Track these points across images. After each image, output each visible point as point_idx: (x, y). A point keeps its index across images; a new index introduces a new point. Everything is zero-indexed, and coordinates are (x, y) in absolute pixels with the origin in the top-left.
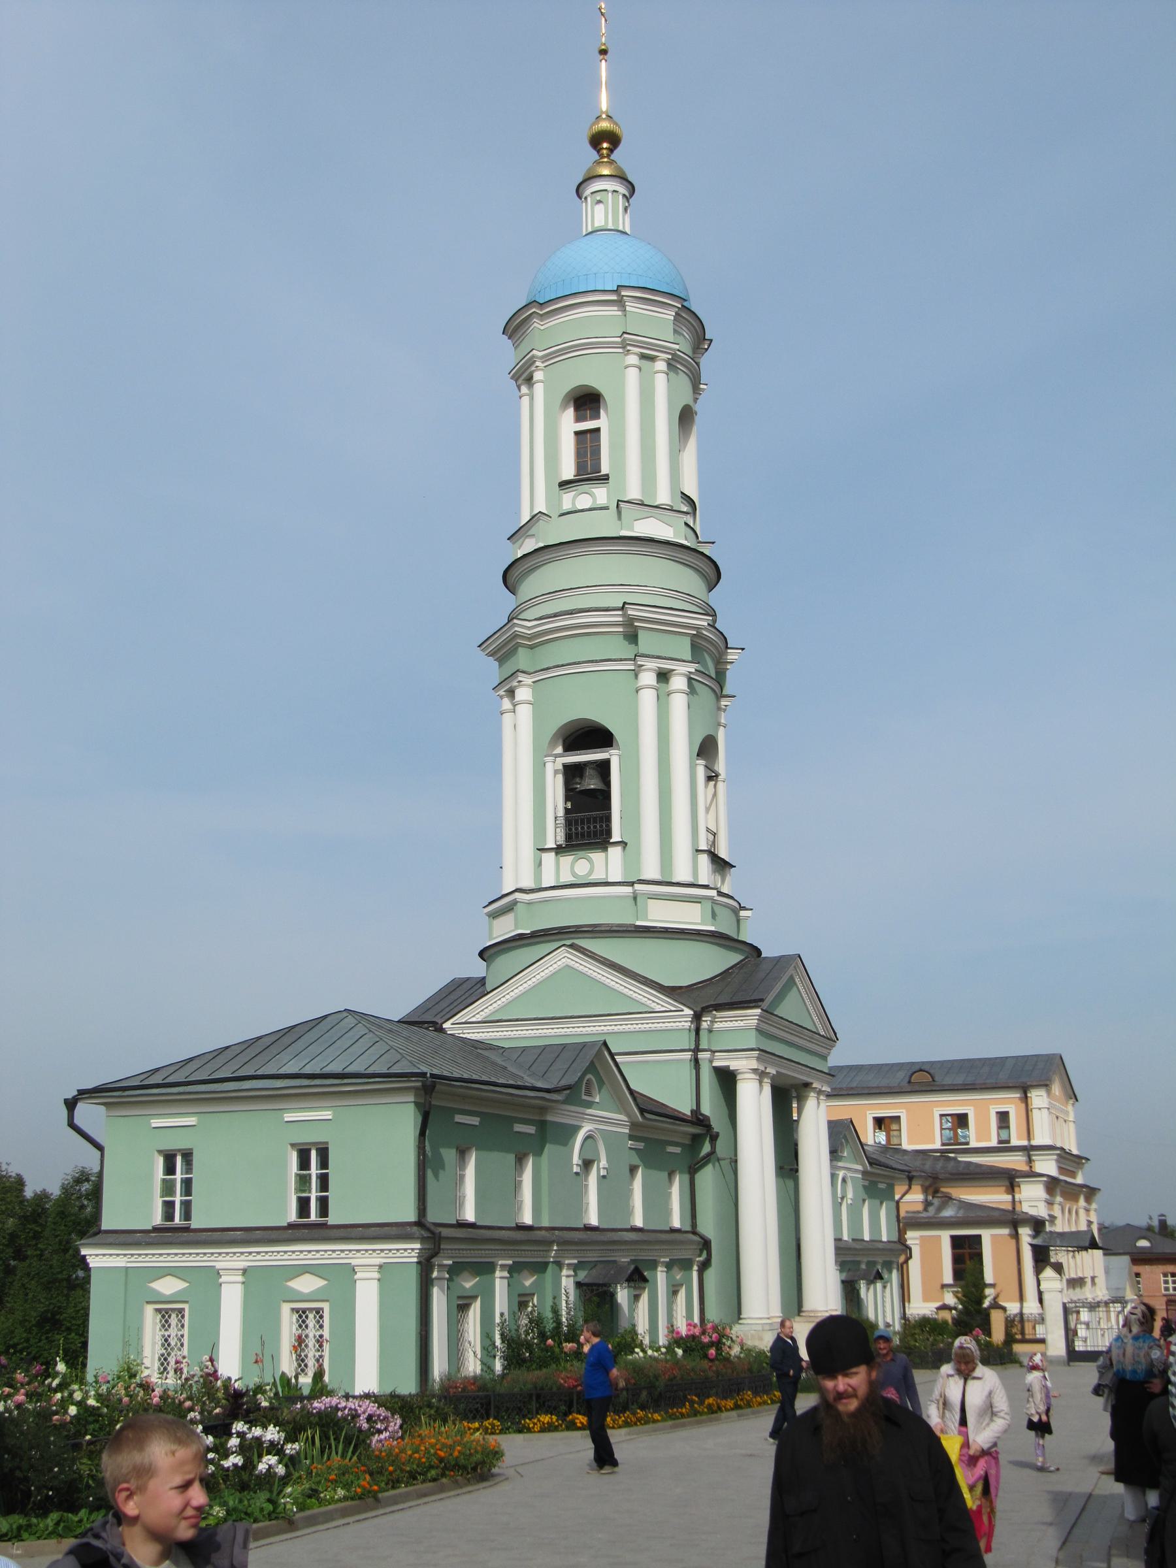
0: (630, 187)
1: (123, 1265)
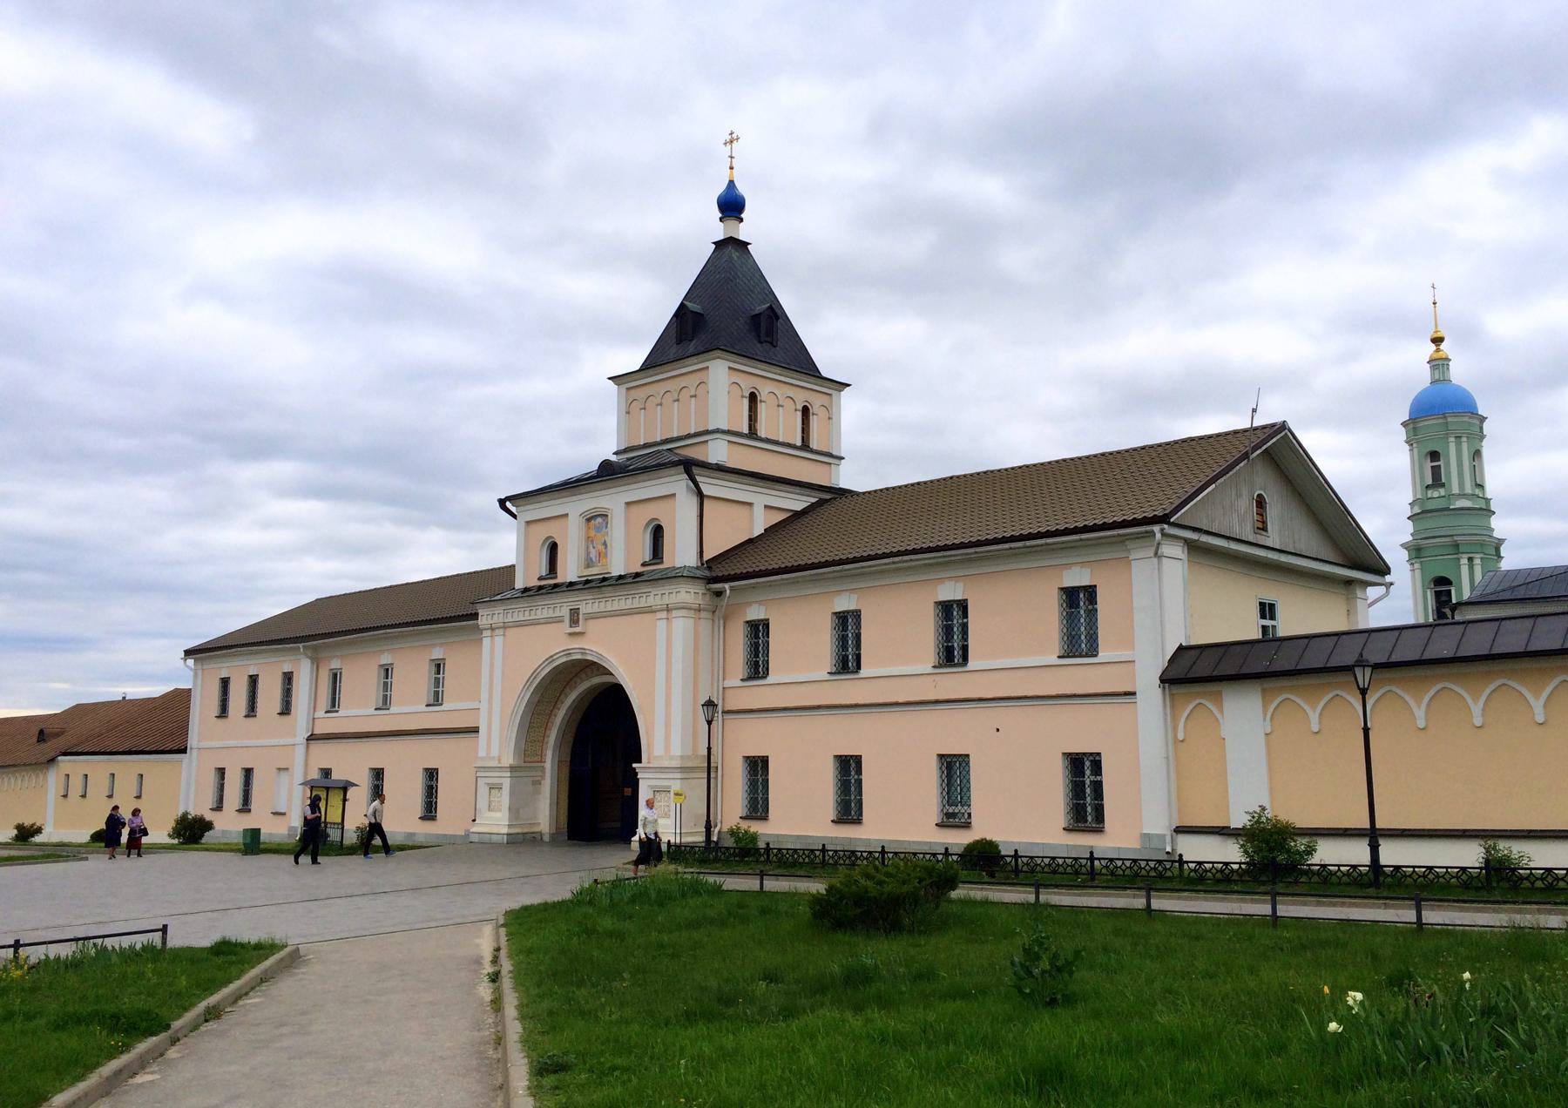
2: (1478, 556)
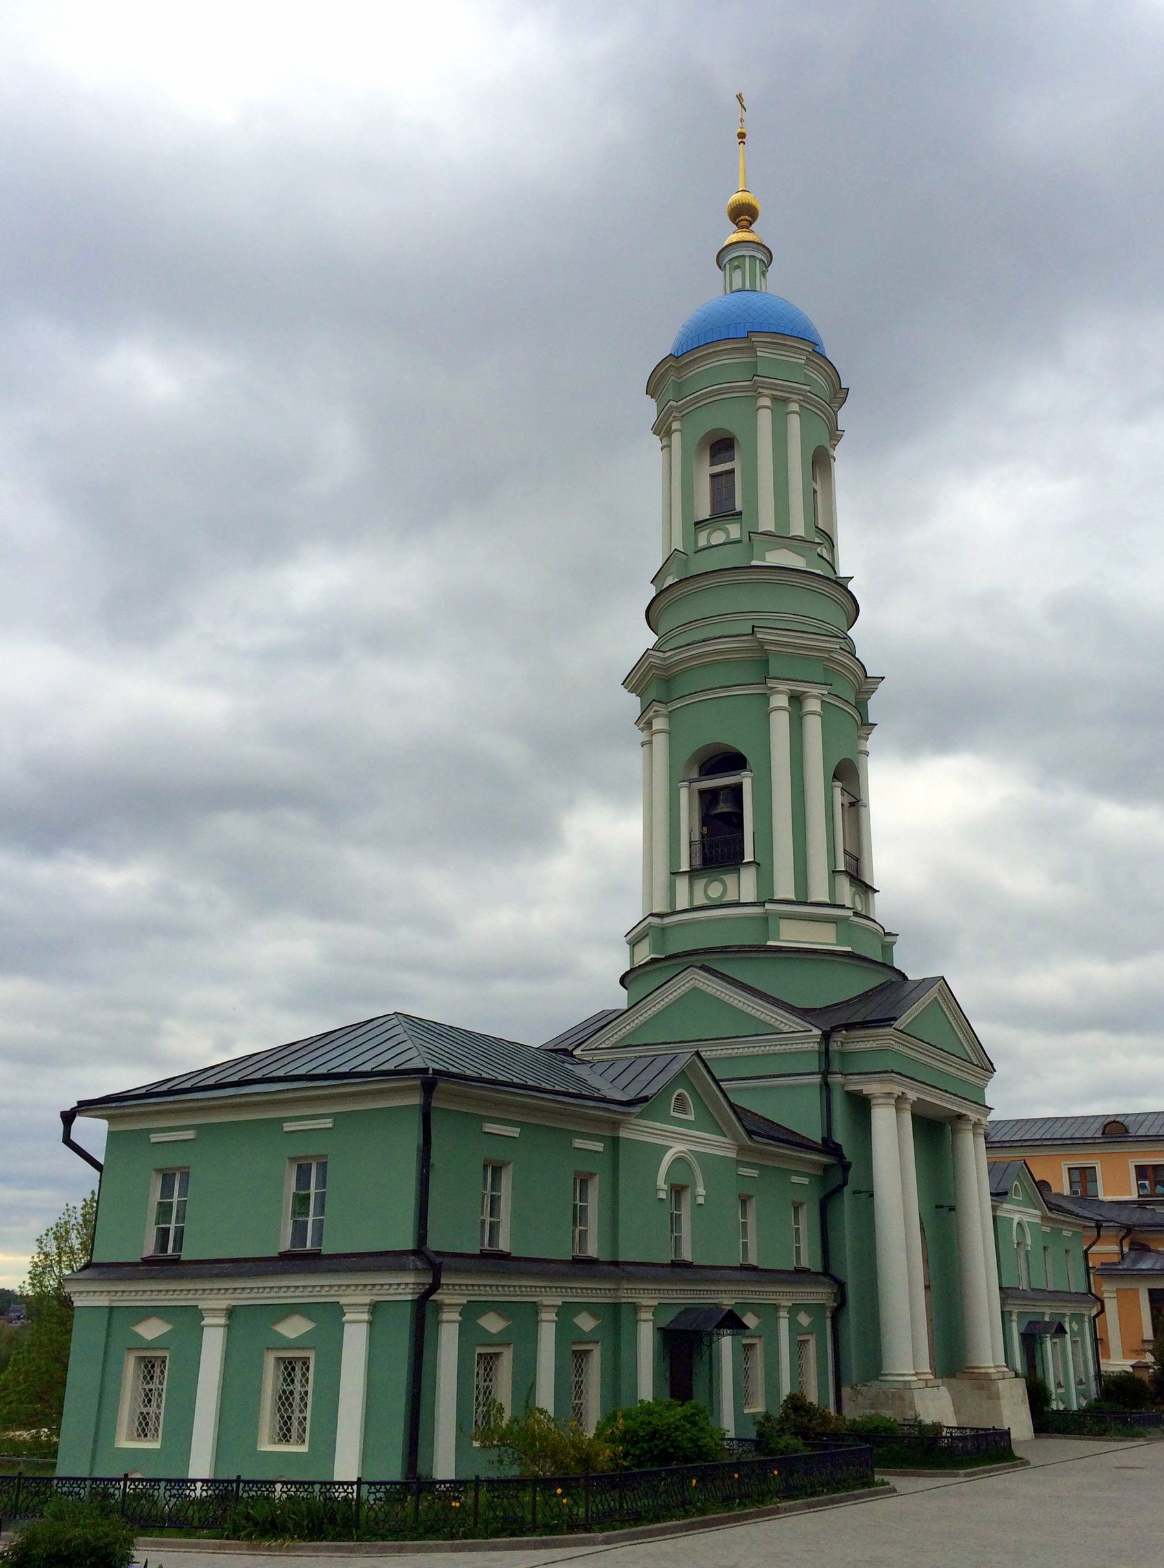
0: (766, 252)
1: (107, 1304)
2: (815, 691)
